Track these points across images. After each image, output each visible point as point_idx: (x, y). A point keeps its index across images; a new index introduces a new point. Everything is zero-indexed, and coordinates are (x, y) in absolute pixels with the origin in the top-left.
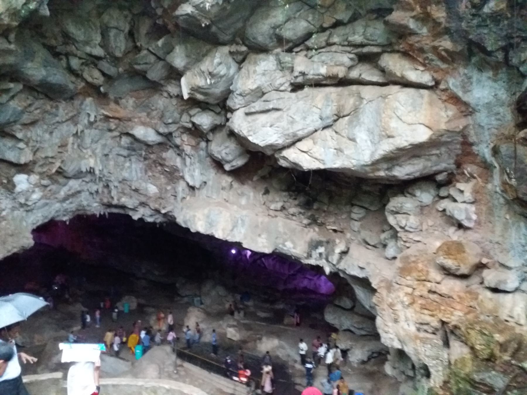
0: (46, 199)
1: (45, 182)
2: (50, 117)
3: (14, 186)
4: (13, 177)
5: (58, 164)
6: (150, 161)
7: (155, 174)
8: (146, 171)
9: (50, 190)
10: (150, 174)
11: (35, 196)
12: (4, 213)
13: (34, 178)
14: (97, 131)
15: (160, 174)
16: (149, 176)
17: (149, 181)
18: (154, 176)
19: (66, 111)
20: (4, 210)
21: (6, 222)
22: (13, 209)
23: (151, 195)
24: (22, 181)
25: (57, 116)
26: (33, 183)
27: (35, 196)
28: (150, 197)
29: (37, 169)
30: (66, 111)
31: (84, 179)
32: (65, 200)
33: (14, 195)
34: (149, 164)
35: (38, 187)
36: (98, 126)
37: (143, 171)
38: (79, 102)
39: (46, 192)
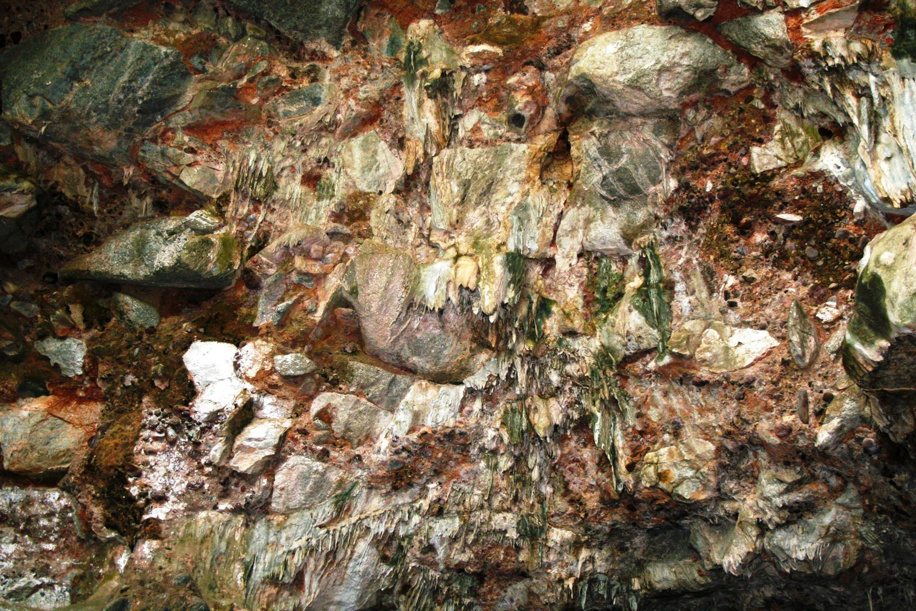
0: (308, 450)
1: (292, 362)
2: (294, 109)
3: (190, 392)
4: (186, 348)
5: (334, 282)
6: (714, 216)
7: (749, 273)
8: (709, 275)
9: (325, 415)
10: (731, 280)
11: (263, 433)
12: (158, 512)
13: (254, 353)
14: (477, 150)
15: (777, 264)
16: (727, 295)
17: (733, 316)
18: (748, 281)
19: (345, 82)
20: (161, 499)
21: (155, 544)
22: (195, 500)
23: (750, 372)
24: (216, 370)
25: (316, 101)
26: (252, 374)
27: (263, 433)
28: (749, 383)
29: (265, 317)
30: (345, 82)
31: (469, 382)
32: (399, 476)
33: (192, 433)
34: (712, 230)
35: (271, 389)
36: (476, 129)
37: (697, 281)
38: (386, 41)
39: (305, 420)
